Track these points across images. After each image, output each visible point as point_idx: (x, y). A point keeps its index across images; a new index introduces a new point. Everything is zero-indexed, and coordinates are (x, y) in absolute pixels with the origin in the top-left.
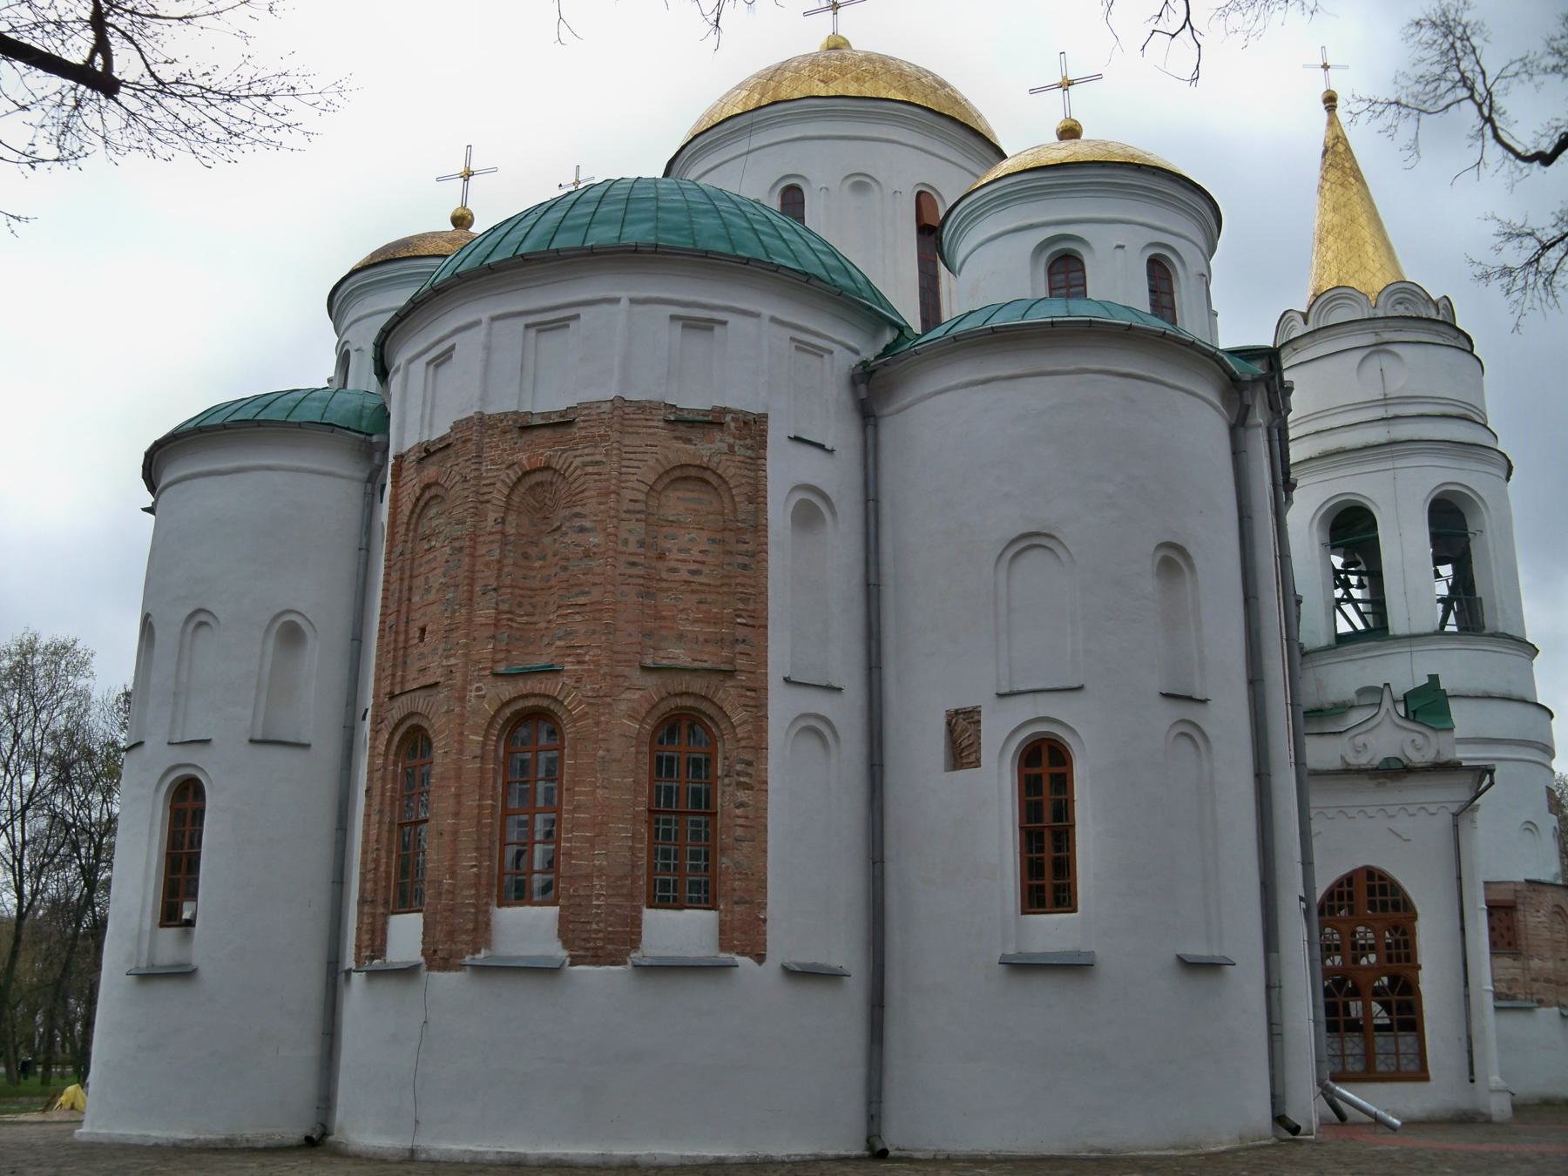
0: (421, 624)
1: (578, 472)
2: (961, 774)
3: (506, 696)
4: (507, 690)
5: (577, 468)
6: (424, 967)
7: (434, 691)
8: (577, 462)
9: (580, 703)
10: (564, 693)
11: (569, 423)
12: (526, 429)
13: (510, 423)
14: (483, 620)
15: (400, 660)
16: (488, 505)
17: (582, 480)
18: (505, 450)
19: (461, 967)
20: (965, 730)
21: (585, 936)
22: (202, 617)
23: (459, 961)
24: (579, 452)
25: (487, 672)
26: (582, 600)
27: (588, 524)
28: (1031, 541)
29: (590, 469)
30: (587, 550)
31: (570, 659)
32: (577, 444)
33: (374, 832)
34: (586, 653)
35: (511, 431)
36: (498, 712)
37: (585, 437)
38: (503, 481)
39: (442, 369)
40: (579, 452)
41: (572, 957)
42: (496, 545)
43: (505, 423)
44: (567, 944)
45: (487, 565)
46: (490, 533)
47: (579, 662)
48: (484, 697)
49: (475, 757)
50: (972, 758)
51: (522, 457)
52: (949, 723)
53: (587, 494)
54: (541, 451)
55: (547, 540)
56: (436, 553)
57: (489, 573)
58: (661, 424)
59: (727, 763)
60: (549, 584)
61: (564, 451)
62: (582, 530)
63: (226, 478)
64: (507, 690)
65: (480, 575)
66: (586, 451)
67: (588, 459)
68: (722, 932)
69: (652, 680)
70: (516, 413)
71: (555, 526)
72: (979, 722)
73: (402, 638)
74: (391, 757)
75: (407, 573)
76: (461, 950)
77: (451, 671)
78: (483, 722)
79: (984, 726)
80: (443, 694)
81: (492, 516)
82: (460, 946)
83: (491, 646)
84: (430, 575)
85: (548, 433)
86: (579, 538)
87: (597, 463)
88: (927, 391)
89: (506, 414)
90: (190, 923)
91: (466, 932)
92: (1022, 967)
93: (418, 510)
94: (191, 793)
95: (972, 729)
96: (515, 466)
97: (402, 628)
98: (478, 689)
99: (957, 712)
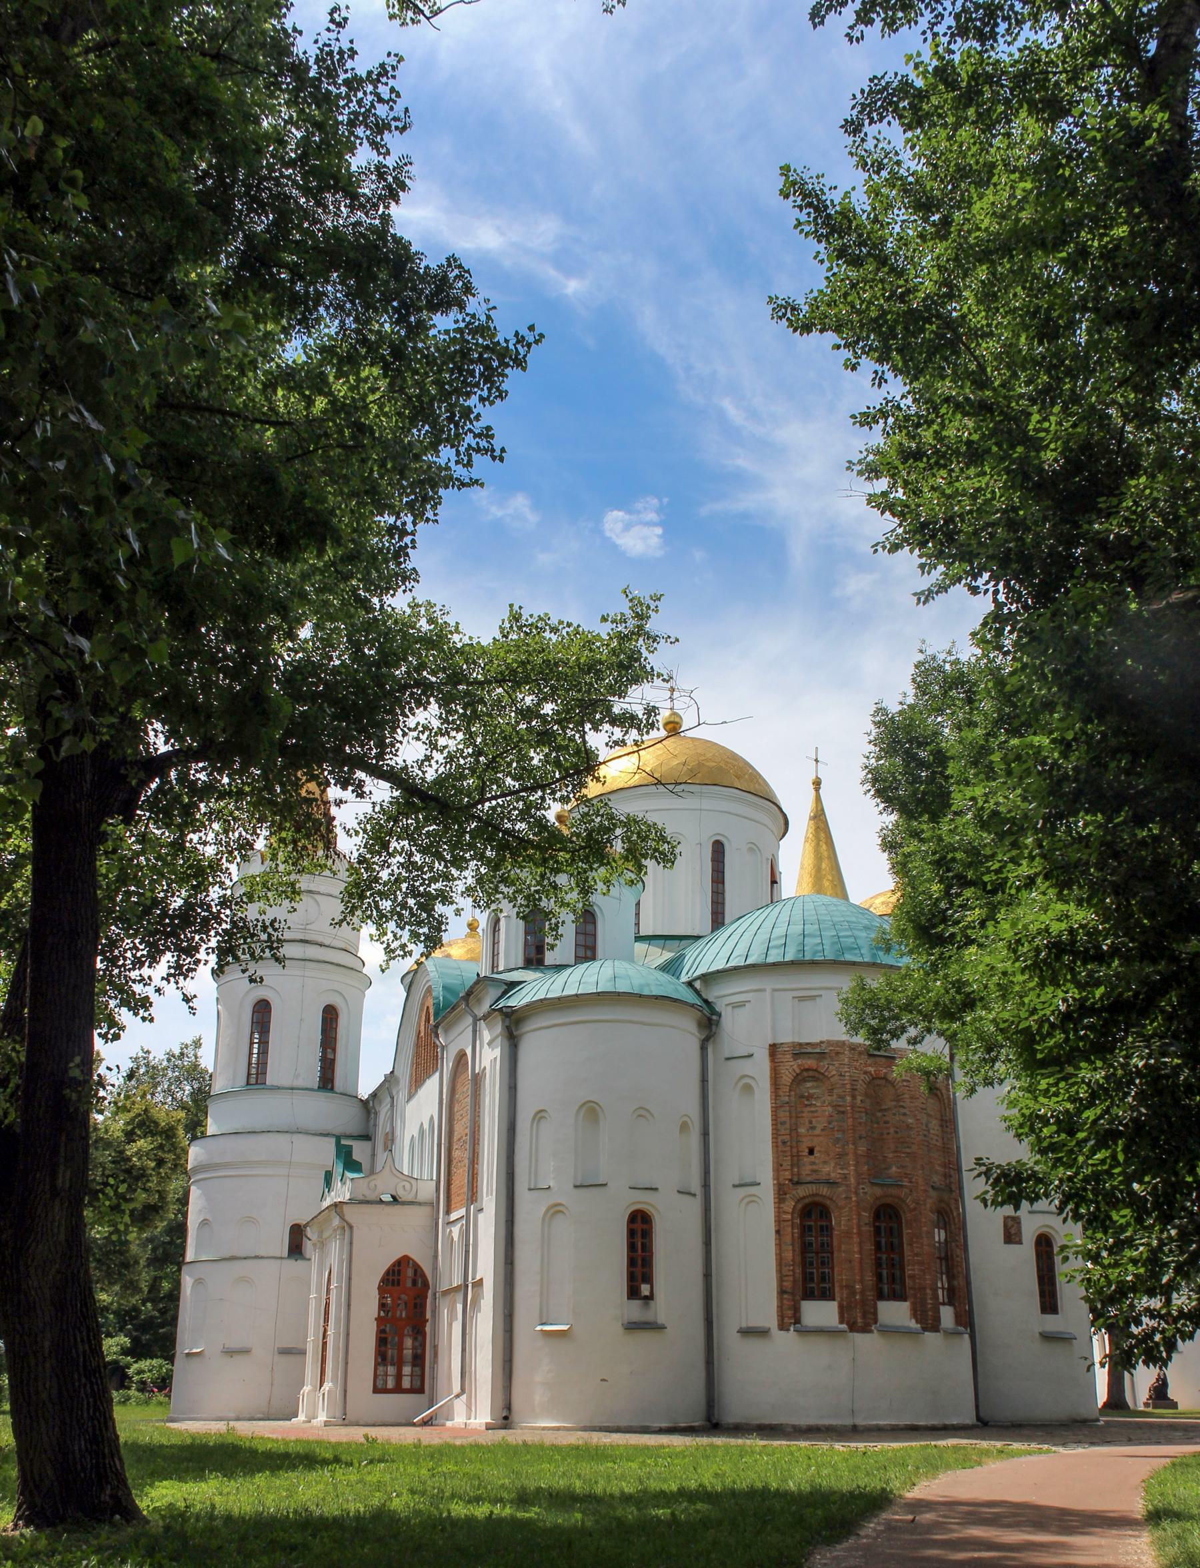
4: (878, 1191)
19: (870, 1331)
22: (642, 1112)
26: (908, 1150)
33: (789, 1255)
44: (917, 1322)
51: (872, 1069)
55: (879, 1114)
62: (905, 1114)
64: (878, 1191)
69: (933, 1193)
73: (795, 1150)
81: (859, 1098)
85: (884, 1060)
90: (650, 1297)
92: (1048, 1338)
94: (639, 1219)
97: (794, 1144)
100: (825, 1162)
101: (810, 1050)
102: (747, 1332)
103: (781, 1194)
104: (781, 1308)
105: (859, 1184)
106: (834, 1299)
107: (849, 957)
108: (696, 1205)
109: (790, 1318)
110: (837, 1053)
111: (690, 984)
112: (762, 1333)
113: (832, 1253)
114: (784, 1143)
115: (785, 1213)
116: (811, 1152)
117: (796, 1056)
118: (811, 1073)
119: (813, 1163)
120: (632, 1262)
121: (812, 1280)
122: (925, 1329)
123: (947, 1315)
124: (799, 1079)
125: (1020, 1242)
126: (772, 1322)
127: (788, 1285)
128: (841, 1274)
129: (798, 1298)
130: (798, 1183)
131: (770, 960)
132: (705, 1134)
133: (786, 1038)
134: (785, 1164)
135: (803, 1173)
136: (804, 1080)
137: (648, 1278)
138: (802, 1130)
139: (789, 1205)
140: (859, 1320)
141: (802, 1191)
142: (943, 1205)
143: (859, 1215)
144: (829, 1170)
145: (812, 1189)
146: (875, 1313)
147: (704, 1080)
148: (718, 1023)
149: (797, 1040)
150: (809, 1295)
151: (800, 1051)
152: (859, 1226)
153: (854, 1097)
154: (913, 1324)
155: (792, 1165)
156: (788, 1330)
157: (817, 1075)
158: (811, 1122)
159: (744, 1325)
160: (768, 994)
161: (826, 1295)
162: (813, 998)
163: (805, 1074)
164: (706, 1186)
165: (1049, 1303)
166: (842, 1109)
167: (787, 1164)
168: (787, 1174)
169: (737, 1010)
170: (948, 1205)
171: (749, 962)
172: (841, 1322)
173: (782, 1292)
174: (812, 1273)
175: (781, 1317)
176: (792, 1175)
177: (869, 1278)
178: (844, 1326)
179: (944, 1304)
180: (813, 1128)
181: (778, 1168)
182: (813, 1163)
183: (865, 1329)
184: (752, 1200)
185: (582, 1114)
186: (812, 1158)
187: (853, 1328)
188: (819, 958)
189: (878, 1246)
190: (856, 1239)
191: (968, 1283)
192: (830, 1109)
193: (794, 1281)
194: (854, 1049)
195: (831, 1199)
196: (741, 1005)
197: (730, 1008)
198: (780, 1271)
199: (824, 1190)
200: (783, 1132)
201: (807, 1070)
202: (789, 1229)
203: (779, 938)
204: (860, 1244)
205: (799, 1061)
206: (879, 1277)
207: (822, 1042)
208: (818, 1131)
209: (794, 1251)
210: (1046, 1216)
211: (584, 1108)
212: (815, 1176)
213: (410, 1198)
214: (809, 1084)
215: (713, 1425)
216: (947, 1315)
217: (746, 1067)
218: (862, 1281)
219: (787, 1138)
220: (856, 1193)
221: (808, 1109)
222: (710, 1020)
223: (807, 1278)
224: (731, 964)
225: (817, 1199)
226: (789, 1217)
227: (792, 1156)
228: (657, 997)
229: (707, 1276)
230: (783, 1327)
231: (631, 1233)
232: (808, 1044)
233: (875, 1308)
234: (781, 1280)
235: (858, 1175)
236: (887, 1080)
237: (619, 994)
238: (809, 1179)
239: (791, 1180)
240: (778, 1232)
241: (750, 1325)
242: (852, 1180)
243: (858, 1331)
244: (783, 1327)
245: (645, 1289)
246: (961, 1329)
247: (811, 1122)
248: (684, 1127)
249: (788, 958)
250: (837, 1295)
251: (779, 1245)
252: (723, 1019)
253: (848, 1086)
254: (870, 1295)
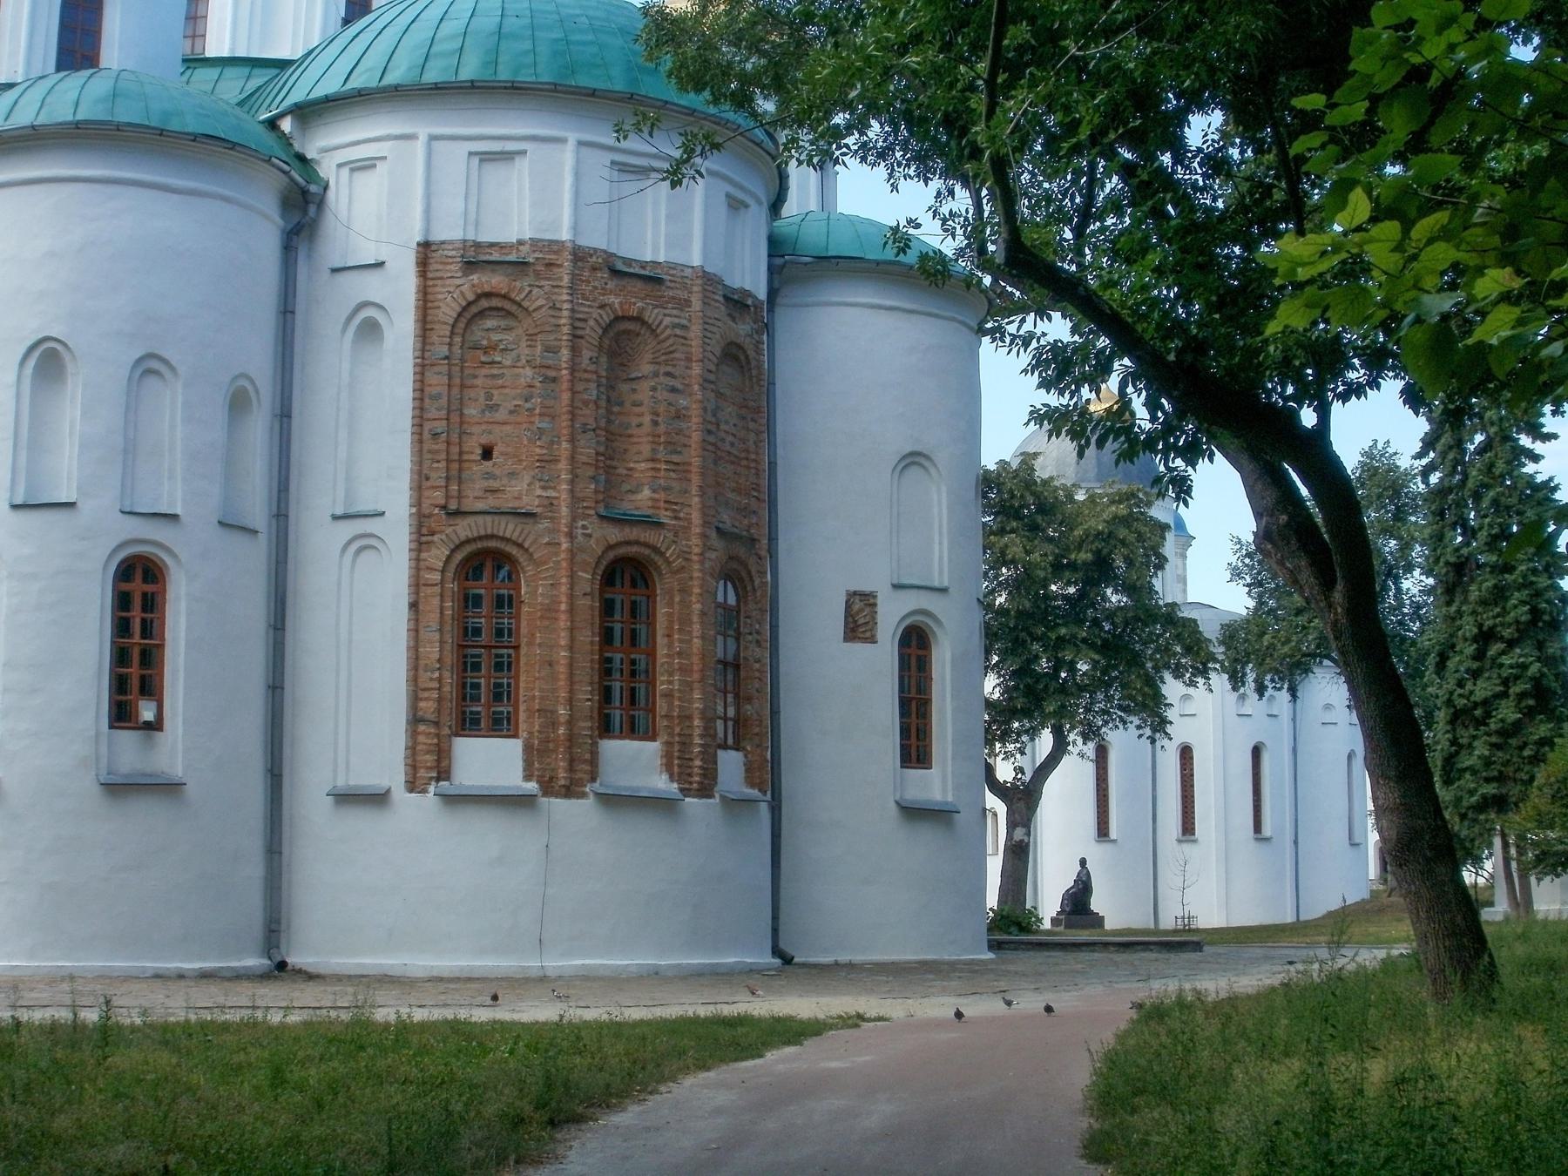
0: (484, 440)
1: (668, 332)
2: (858, 647)
3: (613, 539)
4: (614, 534)
5: (667, 327)
6: (540, 794)
7: (531, 521)
8: (667, 320)
9: (678, 557)
10: (665, 545)
11: (657, 281)
12: (615, 273)
13: (600, 260)
14: (584, 459)
15: (454, 473)
16: (583, 341)
17: (671, 341)
18: (596, 288)
19: (583, 795)
20: (861, 610)
21: (689, 771)
22: (155, 365)
23: (577, 789)
24: (667, 311)
25: (592, 512)
26: (675, 458)
27: (680, 387)
28: (914, 460)
29: (678, 332)
30: (678, 411)
31: (668, 513)
32: (667, 302)
33: (431, 652)
34: (680, 511)
35: (600, 269)
36: (603, 552)
37: (673, 298)
38: (596, 320)
39: (490, 168)
40: (667, 311)
41: (682, 790)
42: (593, 386)
43: (594, 259)
44: (672, 779)
45: (586, 403)
46: (585, 371)
47: (676, 518)
48: (590, 536)
49: (585, 594)
50: (868, 634)
51: (615, 300)
52: (848, 606)
53: (676, 355)
54: (633, 300)
56: (505, 371)
57: (588, 412)
58: (721, 299)
59: (748, 621)
60: (629, 432)
61: (657, 306)
62: (673, 390)
63: (175, 197)
64: (614, 534)
65: (580, 412)
66: (675, 312)
67: (677, 321)
68: (747, 771)
70: (605, 252)
71: (633, 376)
72: (875, 605)
73: (455, 450)
74: (450, 575)
75: (457, 381)
76: (581, 779)
77: (552, 504)
78: (592, 561)
79: (880, 609)
80: (545, 524)
81: (587, 354)
82: (579, 775)
83: (593, 486)
84: (495, 392)
85: (640, 284)
86: (671, 397)
87: (684, 327)
88: (835, 299)
89: (595, 250)
90: (156, 726)
91: (585, 761)
93: (468, 315)
95: (867, 610)
96: (608, 308)
97: (455, 437)
98: (584, 527)
99: (855, 593)
100: (512, 475)
101: (496, 257)
102: (347, 798)
103: (422, 536)
104: (412, 750)
105: (574, 519)
106: (515, 736)
107: (584, 81)
108: (254, 556)
110: (550, 265)
111: (272, 124)
112: (377, 799)
113: (517, 648)
114: (435, 435)
115: (431, 569)
116: (487, 453)
117: (470, 266)
118: (495, 302)
119: (489, 476)
120: (121, 656)
121: (476, 699)
122: (685, 792)
123: (731, 765)
124: (475, 311)
125: (872, 640)
127: (428, 707)
128: (530, 684)
129: (446, 731)
130: (458, 513)
131: (431, 76)
132: (284, 415)
133: (450, 230)
134: (433, 475)
135: (469, 493)
136: (481, 314)
137: (151, 688)
138: (472, 411)
139: (437, 556)
140: (562, 774)
141: (464, 529)
142: (735, 565)
143: (572, 576)
144: (523, 491)
146: (594, 761)
147: (287, 310)
148: (321, 203)
149: (471, 236)
150: (468, 725)
151: (475, 258)
152: (571, 597)
153: (574, 350)
154: (662, 784)
155: (448, 479)
156: (424, 791)
157: (507, 305)
158: (489, 397)
159: (341, 782)
160: (420, 146)
161: (500, 726)
163: (484, 303)
164: (281, 515)
165: (915, 750)
166: (552, 373)
167: (438, 477)
168: (439, 496)
169: (358, 176)
170: (744, 564)
171: (386, 81)
172: (528, 778)
173: (415, 720)
174: (476, 686)
175: (413, 766)
176: (447, 497)
177: (586, 695)
178: (532, 787)
179: (725, 747)
180: (493, 408)
182: (489, 476)
183: (570, 791)
184: (365, 545)
185: (32, 363)
186: (489, 464)
187: (548, 788)
188: (525, 77)
189: (607, 636)
190: (563, 622)
191: (775, 713)
192: (529, 372)
193: (440, 700)
194: (582, 259)
195: (520, 546)
196: (367, 165)
197: (345, 171)
198: (414, 680)
199: (509, 528)
200: (433, 413)
201: (488, 295)
202: (436, 601)
203: (453, 37)
204: (572, 630)
205: (475, 277)
206: (606, 695)
207: (521, 243)
208: (501, 415)
209: (442, 642)
210: (922, 592)
211: (37, 354)
212: (490, 503)
214: (490, 323)
216: (731, 765)
217: (370, 287)
218: (570, 702)
219: (440, 426)
220: (571, 535)
221: (484, 371)
222: (305, 193)
223: (466, 692)
224: (356, 83)
225: (493, 544)
226: (437, 577)
227: (448, 461)
228: (194, 137)
229: (276, 687)
230: (413, 786)
231: (122, 601)
232: (492, 245)
233: (594, 754)
234: (415, 698)
235: (575, 499)
236: (644, 323)
237: (119, 127)
238: (480, 506)
239: (444, 507)
240: (414, 606)
241: (352, 783)
242: (564, 510)
243: (557, 795)
244: (413, 786)
245: (147, 713)
246: (754, 793)
247: (489, 397)
248: (238, 403)
249: (466, 74)
250: (522, 726)
251: (415, 631)
252: (331, 195)
253: (566, 330)
254: (585, 726)
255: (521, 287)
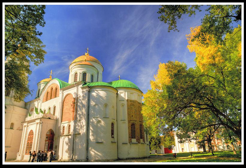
4: (140, 122)
102: (123, 144)
109: (130, 142)
112: (127, 144)
116: (132, 116)
126: (128, 143)
139: (130, 124)
144: (135, 119)
145: (133, 122)
150: (132, 138)
151: (131, 101)
162: (132, 94)
181: (128, 118)
199: (135, 122)
213: (53, 118)
215: (119, 160)
230: (129, 143)
234: (129, 135)
255: (134, 103)
